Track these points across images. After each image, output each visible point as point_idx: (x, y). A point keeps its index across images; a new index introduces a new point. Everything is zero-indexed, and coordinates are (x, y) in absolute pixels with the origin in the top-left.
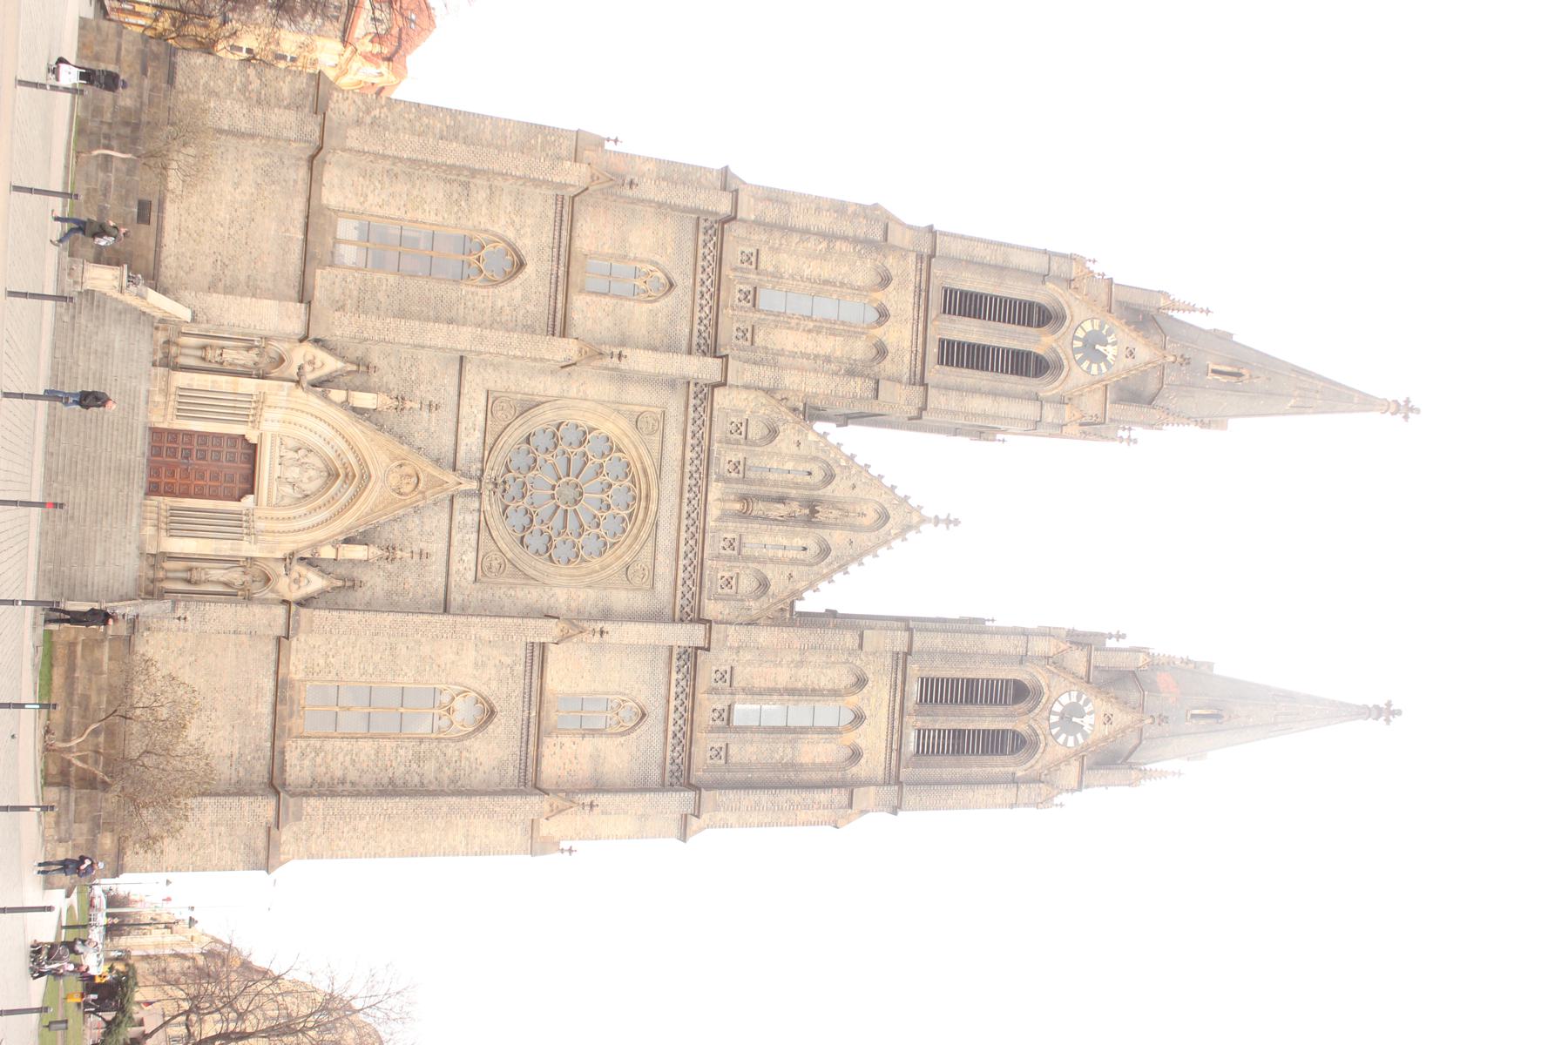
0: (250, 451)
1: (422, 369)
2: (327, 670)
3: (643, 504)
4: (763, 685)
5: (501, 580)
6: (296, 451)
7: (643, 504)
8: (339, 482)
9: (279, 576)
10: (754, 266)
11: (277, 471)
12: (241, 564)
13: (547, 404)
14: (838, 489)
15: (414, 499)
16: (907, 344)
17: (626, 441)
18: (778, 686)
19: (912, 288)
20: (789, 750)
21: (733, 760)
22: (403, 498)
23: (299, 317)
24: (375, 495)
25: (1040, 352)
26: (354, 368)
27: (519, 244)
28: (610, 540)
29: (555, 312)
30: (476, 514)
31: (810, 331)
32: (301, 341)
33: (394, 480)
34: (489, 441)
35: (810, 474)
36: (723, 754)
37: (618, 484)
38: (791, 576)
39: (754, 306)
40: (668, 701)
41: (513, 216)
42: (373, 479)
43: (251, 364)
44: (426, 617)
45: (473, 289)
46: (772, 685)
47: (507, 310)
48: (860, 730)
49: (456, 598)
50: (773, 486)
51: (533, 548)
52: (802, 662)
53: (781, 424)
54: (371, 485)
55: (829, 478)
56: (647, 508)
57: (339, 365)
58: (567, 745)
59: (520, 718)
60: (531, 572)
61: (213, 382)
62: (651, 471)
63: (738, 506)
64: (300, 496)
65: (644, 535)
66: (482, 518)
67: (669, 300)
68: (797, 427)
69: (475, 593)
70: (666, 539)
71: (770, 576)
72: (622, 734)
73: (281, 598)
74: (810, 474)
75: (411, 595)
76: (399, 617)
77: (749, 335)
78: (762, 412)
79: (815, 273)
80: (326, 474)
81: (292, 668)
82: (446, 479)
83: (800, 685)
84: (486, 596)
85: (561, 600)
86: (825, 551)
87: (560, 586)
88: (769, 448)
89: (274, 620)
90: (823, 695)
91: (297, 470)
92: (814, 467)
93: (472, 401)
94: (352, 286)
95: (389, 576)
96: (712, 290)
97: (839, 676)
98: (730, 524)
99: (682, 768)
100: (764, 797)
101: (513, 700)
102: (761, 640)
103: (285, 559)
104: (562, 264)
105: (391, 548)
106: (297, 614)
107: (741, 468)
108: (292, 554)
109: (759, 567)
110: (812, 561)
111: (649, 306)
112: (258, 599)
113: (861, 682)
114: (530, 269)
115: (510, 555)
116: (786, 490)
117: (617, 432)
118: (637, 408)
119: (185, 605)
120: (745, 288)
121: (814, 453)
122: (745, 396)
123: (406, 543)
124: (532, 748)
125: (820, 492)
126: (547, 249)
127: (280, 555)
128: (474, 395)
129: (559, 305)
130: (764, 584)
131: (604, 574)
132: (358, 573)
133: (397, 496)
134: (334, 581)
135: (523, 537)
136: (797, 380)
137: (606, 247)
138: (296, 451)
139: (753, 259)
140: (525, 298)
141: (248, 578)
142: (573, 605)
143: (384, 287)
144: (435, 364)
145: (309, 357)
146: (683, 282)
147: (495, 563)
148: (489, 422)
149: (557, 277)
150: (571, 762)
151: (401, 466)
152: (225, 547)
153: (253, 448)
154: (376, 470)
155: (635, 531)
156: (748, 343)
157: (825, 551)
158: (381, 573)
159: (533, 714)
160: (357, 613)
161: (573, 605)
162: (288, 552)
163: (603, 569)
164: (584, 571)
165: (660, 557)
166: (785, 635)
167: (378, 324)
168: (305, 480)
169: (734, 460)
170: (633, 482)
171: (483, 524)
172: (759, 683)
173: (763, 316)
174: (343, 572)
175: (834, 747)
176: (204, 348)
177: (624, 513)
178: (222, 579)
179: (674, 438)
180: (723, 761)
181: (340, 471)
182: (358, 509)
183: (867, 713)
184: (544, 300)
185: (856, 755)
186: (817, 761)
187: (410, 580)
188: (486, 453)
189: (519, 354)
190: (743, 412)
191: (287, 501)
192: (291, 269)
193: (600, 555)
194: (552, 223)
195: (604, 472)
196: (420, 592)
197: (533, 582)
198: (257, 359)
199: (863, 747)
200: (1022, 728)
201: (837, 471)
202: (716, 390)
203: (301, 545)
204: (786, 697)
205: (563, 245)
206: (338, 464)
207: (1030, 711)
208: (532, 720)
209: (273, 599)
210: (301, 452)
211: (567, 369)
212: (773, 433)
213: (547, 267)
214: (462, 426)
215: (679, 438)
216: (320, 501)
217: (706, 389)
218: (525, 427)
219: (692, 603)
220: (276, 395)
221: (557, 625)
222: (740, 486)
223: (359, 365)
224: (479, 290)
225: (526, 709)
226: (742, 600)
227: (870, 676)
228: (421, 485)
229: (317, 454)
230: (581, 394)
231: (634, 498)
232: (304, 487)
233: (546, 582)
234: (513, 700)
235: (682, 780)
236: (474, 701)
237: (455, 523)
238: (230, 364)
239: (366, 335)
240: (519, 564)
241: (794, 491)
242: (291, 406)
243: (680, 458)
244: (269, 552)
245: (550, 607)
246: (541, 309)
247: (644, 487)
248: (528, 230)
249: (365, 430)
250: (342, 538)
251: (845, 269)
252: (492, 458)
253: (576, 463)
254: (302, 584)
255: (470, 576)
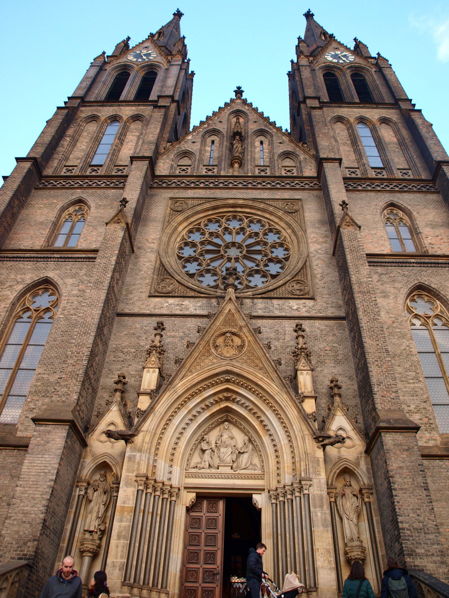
0: (205, 503)
1: (126, 344)
2: (423, 411)
3: (239, 209)
4: (354, 155)
5: (310, 283)
6: (203, 451)
7: (239, 209)
8: (234, 407)
9: (340, 459)
10: (75, 168)
11: (228, 470)
12: (333, 500)
13: (162, 259)
14: (223, 127)
15: (247, 334)
16: (134, 108)
17: (192, 219)
18: (352, 149)
19: (101, 108)
20: (391, 146)
21: (407, 167)
22: (247, 344)
23: (49, 432)
24: (245, 366)
25: (144, 73)
26: (118, 394)
27: (29, 281)
28: (267, 227)
29: (89, 258)
30: (256, 301)
31: (122, 144)
32: (84, 444)
33: (230, 352)
34: (192, 294)
35: (213, 142)
36: (405, 171)
37: (224, 224)
38: (281, 143)
39: (101, 166)
40: (379, 191)
41: (5, 287)
42: (229, 368)
43: (104, 498)
44: (360, 314)
45: (60, 310)
46: (352, 153)
47: (81, 287)
48: (370, 118)
49: (330, 312)
50: (222, 151)
51: (280, 270)
52: (334, 138)
53: (180, 150)
54: (235, 370)
55: (215, 132)
56: (241, 206)
57: (115, 409)
58: (430, 241)
59: (419, 268)
60: (300, 265)
61: (119, 537)
62: (214, 204)
63: (236, 165)
64: (251, 446)
65: (262, 206)
66: (260, 296)
67: (91, 201)
68: (182, 143)
69: (325, 300)
70: (265, 195)
71: (281, 151)
72: (409, 214)
73: (364, 455)
74: (213, 142)
75: (334, 345)
76: (365, 334)
77: (121, 168)
78: (172, 157)
79: (85, 144)
80: (227, 423)
81: (431, 444)
82: (227, 311)
83: (349, 142)
84: (325, 292)
85: (319, 247)
86: (261, 132)
87: (308, 248)
88: (197, 154)
89: (401, 445)
90: (353, 131)
91: (222, 450)
92: (209, 140)
93: (157, 307)
94: (39, 403)
95: (322, 363)
96: (87, 181)
97: (340, 128)
98: (249, 167)
99: (422, 185)
100: (430, 143)
101: (406, 273)
102: (327, 144)
103: (324, 446)
104: (52, 256)
105: (296, 355)
106: (388, 421)
107: (210, 168)
108: (317, 439)
109: (276, 157)
110: (269, 137)
111: (92, 209)
112: (369, 478)
113: (340, 119)
114: (51, 274)
115: (288, 278)
116: (225, 146)
117: (185, 224)
118: (168, 212)
119: (410, 555)
120: (89, 170)
121: (201, 136)
122: (162, 164)
123: (288, 350)
124: (440, 261)
125: (225, 133)
126: (37, 265)
127: (320, 453)
128: (152, 306)
129: (83, 256)
130: (287, 155)
131: (294, 225)
132: (324, 389)
133: (245, 349)
134: (336, 404)
135: (271, 275)
136: (151, 136)
137: (44, 232)
138: (203, 451)
139: (70, 168)
140: (73, 276)
141: (348, 491)
142: (321, 240)
143: (45, 376)
144: (122, 334)
145: (104, 437)
146: (78, 194)
147: (297, 287)
148: (176, 295)
149: (61, 258)
150: (442, 239)
151: (216, 347)
152: (319, 514)
153: (200, 497)
154: (220, 366)
155: (259, 213)
156: (126, 168)
157: (261, 132)
158: (319, 369)
159: (413, 260)
160: (370, 369)
161: (321, 240)
162: (316, 445)
163: (289, 225)
164: (294, 238)
165: (278, 197)
166: (321, 135)
167: (71, 361)
168: (233, 443)
169: (205, 171)
170: (222, 217)
171: (264, 296)
172: (353, 157)
173: (109, 159)
174: (325, 401)
175: (382, 130)
176: (82, 552)
177: (246, 221)
178: (355, 520)
179: (190, 193)
180: (410, 171)
181: (223, 405)
182: (261, 379)
183: (358, 115)
184: (78, 264)
185: (384, 121)
186: (394, 135)
187: (322, 346)
188: (202, 295)
189: (115, 258)
190: (172, 166)
191: (256, 461)
192: (10, 460)
193: (278, 232)
194: (17, 263)
195: (216, 231)
196: (331, 338)
197: (308, 263)
198: (100, 490)
199: (379, 117)
200: (348, 73)
201: (210, 128)
202: (158, 173)
203: (306, 432)
204: (359, 143)
205: (35, 255)
206: (215, 409)
207: (339, 69)
208: (419, 261)
209: (367, 464)
210: (204, 446)
211: (135, 249)
212: (186, 154)
213: (51, 264)
214: (178, 312)
215: (189, 191)
216: (255, 423)
217: (156, 181)
218: (180, 274)
219: (307, 182)
220: (139, 464)
221: (345, 229)
222: (223, 164)
223: (116, 390)
224: (61, 306)
225: (412, 265)
226: (300, 162)
227: (336, 115)
228: (234, 330)
229: (207, 432)
230: (155, 241)
231: (235, 217)
232: (240, 444)
233: (306, 254)
234: (406, 273)
235: (431, 185)
236: (413, 303)
237: (266, 314)
238: (104, 522)
239: (81, 372)
240: (294, 272)
241: (225, 143)
242: (153, 450)
243: (204, 190)
244: (318, 465)
245: (326, 253)
246: (85, 266)
247: (225, 210)
248: (19, 276)
249: (181, 376)
250: (293, 394)
251: (85, 134)
252: (208, 292)
253: (209, 247)
254: (344, 435)
255: (310, 303)
